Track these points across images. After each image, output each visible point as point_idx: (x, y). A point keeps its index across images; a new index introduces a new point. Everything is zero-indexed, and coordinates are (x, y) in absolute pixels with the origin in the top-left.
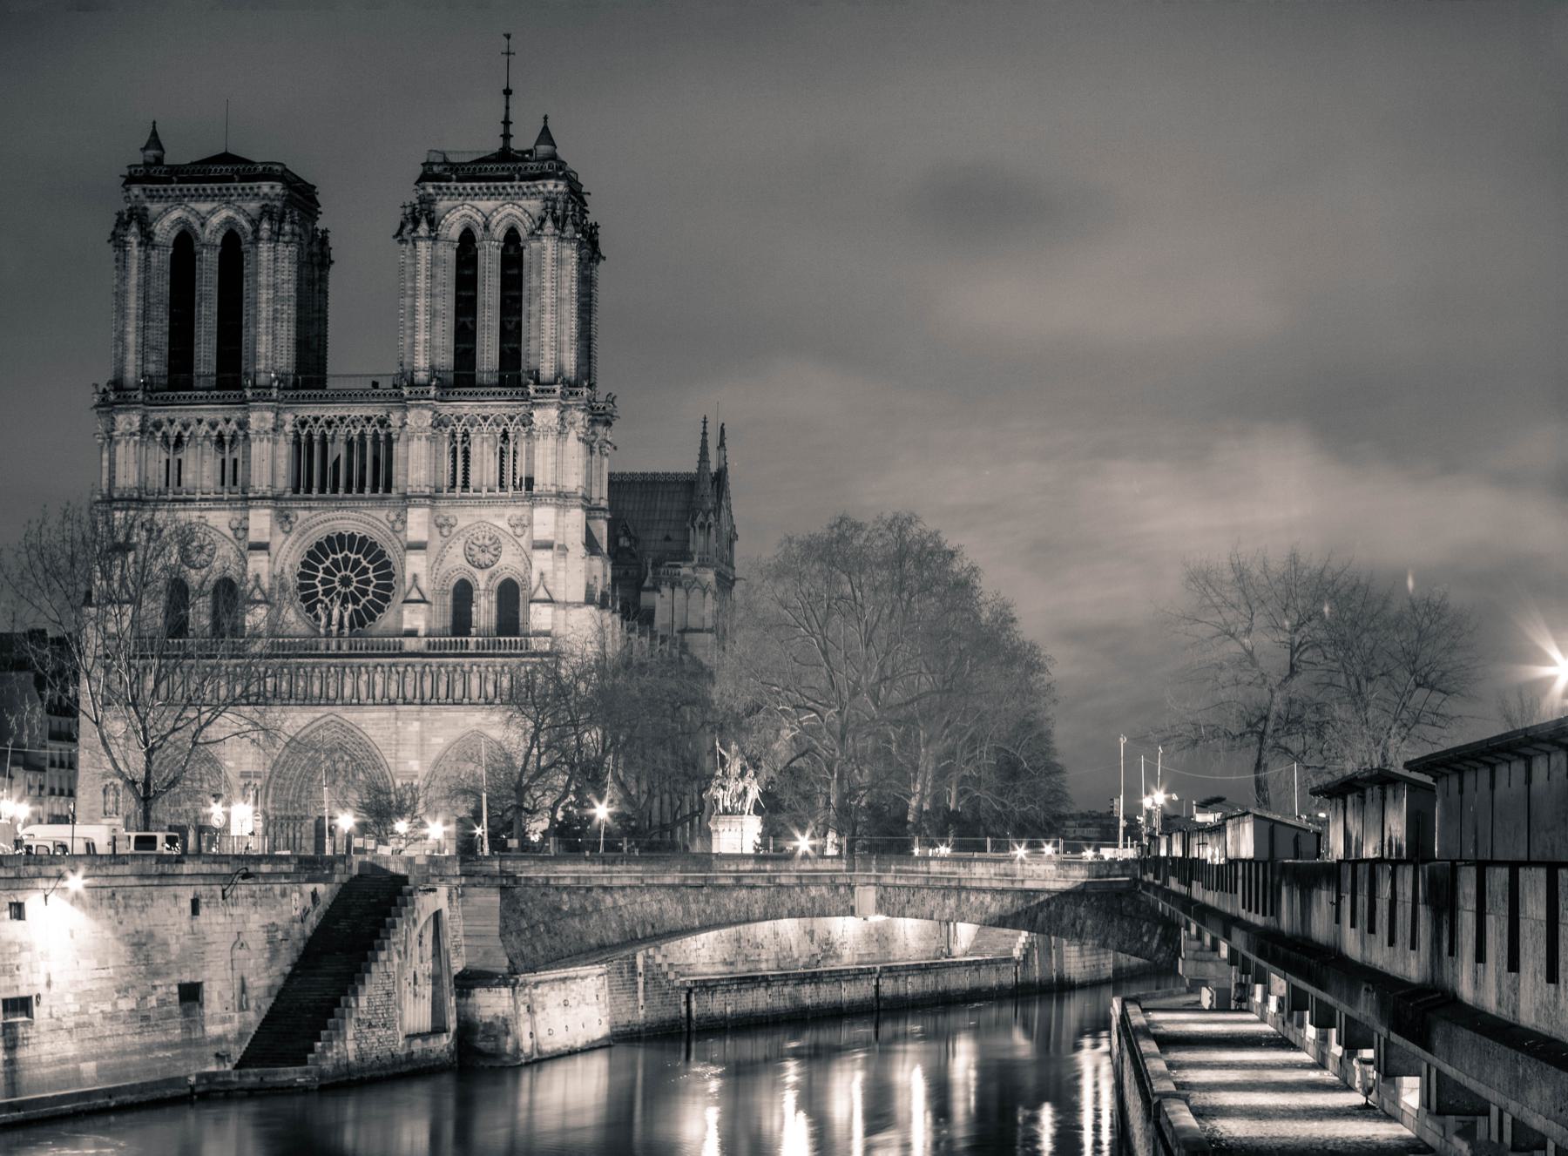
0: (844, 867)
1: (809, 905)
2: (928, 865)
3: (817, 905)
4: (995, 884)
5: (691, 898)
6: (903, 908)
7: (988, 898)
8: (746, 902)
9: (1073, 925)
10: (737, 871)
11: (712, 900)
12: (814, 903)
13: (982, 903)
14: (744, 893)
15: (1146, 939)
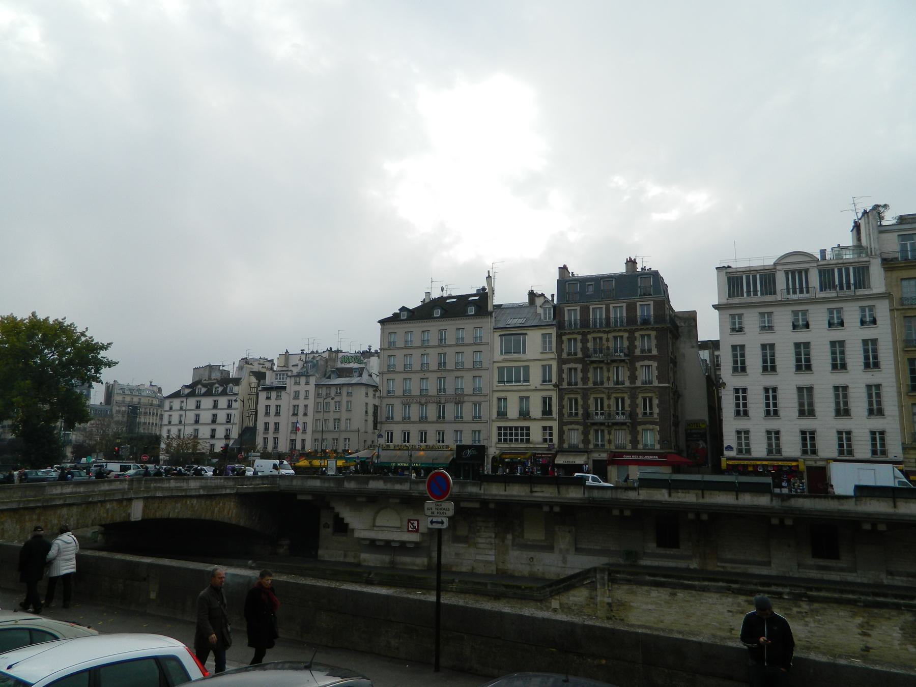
0: (126, 486)
1: (105, 515)
2: (169, 482)
3: (110, 514)
4: (202, 492)
5: (27, 517)
6: (156, 511)
7: (195, 501)
8: (66, 516)
9: (228, 514)
10: (61, 494)
11: (42, 518)
12: (108, 514)
13: (192, 504)
14: (64, 511)
15: (254, 518)
